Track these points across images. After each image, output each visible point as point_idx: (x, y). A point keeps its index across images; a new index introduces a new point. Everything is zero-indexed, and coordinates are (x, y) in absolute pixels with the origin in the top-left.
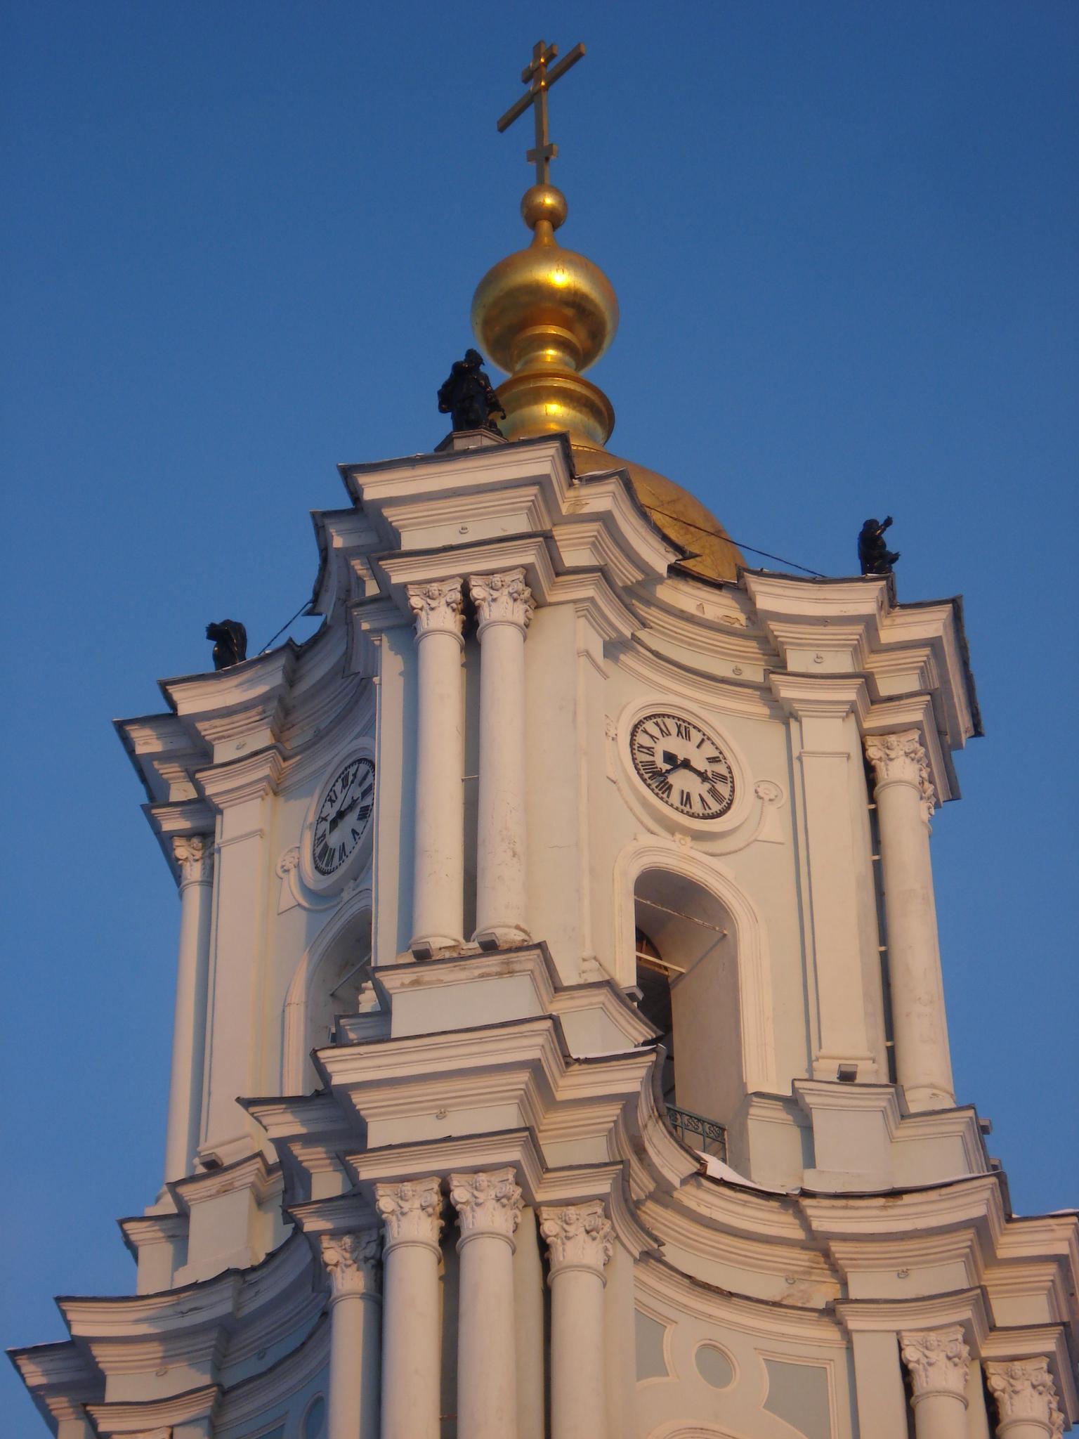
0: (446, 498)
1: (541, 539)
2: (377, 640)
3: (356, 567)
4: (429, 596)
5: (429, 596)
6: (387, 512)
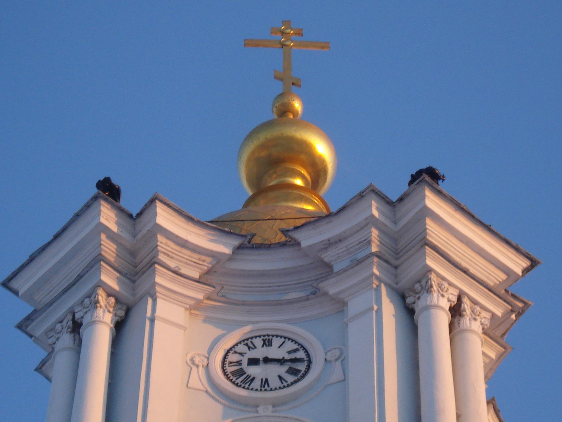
0: (461, 241)
1: (510, 308)
2: (375, 284)
3: (373, 234)
4: (440, 286)
5: (440, 286)
6: (429, 222)
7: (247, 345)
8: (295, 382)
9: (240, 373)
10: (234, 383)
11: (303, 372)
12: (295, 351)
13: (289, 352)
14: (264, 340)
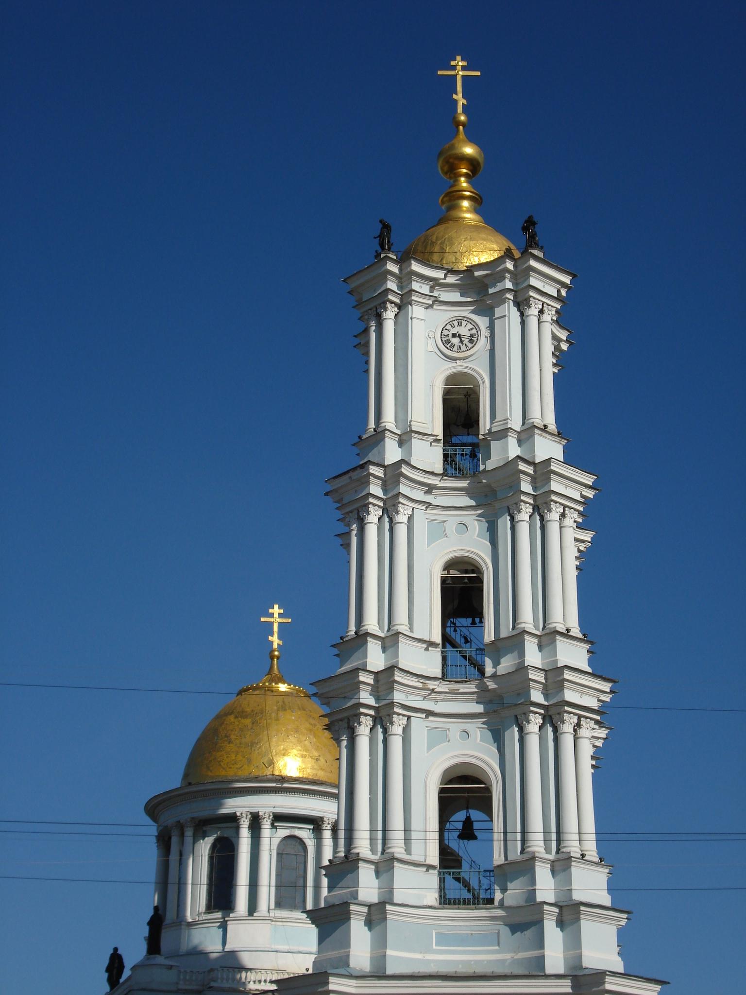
4: (535, 302)
7: (451, 325)
8: (472, 347)
9: (448, 342)
10: (446, 347)
11: (475, 342)
12: (472, 329)
13: (469, 330)
14: (458, 322)
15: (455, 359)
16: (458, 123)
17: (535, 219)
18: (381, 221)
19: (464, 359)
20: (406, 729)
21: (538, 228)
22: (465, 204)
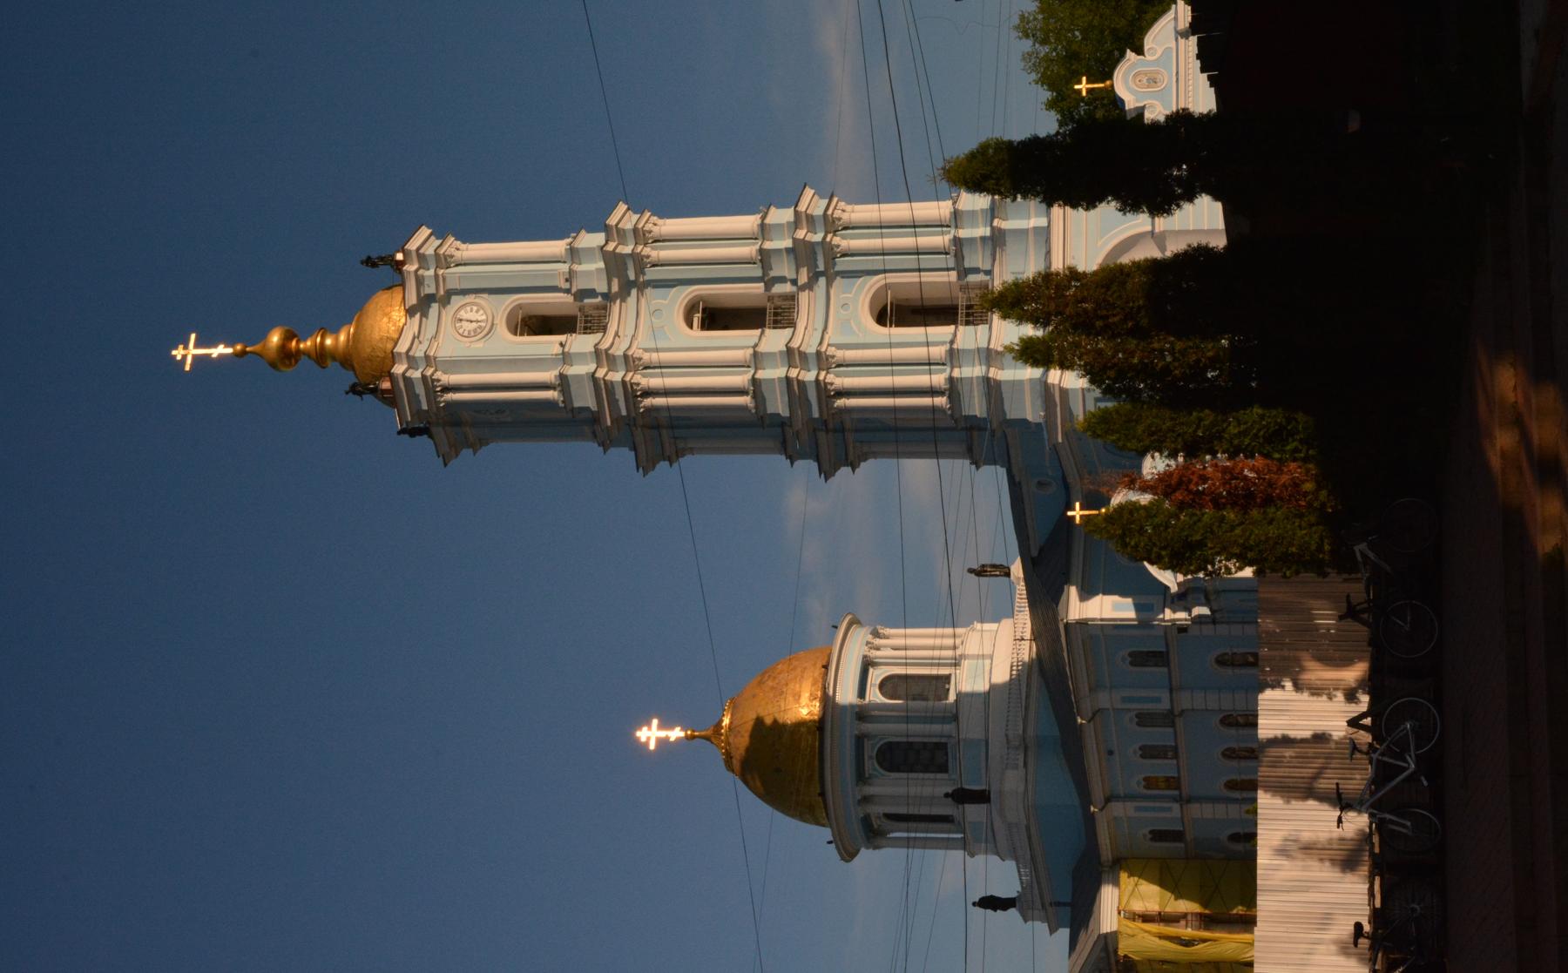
15: (493, 324)
16: (243, 353)
17: (364, 258)
18: (347, 393)
19: (493, 317)
20: (839, 347)
21: (374, 255)
22: (329, 342)
